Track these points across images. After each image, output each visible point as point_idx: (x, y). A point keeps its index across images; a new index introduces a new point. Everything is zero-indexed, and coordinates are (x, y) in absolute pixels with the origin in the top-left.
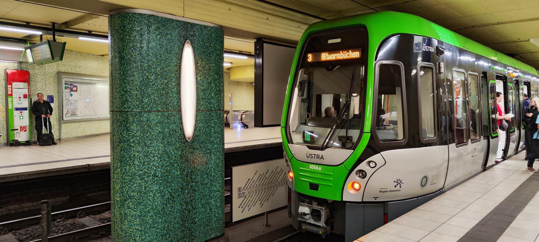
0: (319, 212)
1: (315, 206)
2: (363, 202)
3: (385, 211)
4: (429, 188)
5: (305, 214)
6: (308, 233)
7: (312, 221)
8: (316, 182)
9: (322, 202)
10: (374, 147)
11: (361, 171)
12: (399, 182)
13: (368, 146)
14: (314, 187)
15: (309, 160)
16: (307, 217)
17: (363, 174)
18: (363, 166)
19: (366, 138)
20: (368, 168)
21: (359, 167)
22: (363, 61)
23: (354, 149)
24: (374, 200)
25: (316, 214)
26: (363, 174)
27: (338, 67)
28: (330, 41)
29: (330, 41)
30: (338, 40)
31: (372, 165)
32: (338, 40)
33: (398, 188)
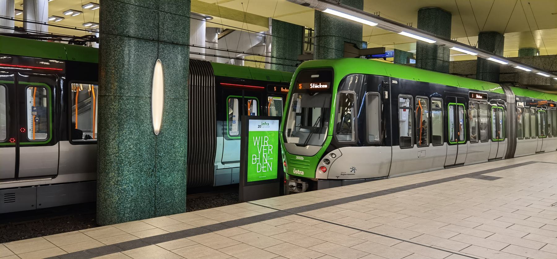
1: (299, 181)
5: (292, 186)
9: (303, 179)
10: (334, 145)
11: (327, 160)
12: (353, 169)
13: (331, 144)
16: (294, 188)
17: (327, 161)
18: (328, 156)
20: (331, 157)
22: (329, 91)
23: (322, 146)
27: (316, 94)
29: (313, 76)
30: (317, 76)
31: (334, 156)
32: (317, 76)
33: (353, 172)
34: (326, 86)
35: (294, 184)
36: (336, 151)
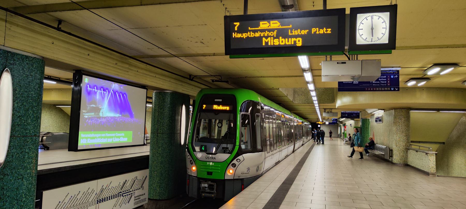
0: (213, 185)
2: (234, 179)
3: (242, 184)
4: (260, 172)
6: (205, 197)
7: (209, 191)
8: (210, 171)
12: (249, 169)
14: (210, 173)
15: (207, 160)
16: (206, 189)
17: (234, 165)
19: (237, 148)
21: (233, 162)
22: (233, 111)
24: (238, 178)
25: (211, 187)
26: (234, 165)
28: (216, 100)
29: (216, 100)
30: (221, 100)
32: (221, 100)
34: (228, 108)
35: (206, 185)
36: (240, 157)
